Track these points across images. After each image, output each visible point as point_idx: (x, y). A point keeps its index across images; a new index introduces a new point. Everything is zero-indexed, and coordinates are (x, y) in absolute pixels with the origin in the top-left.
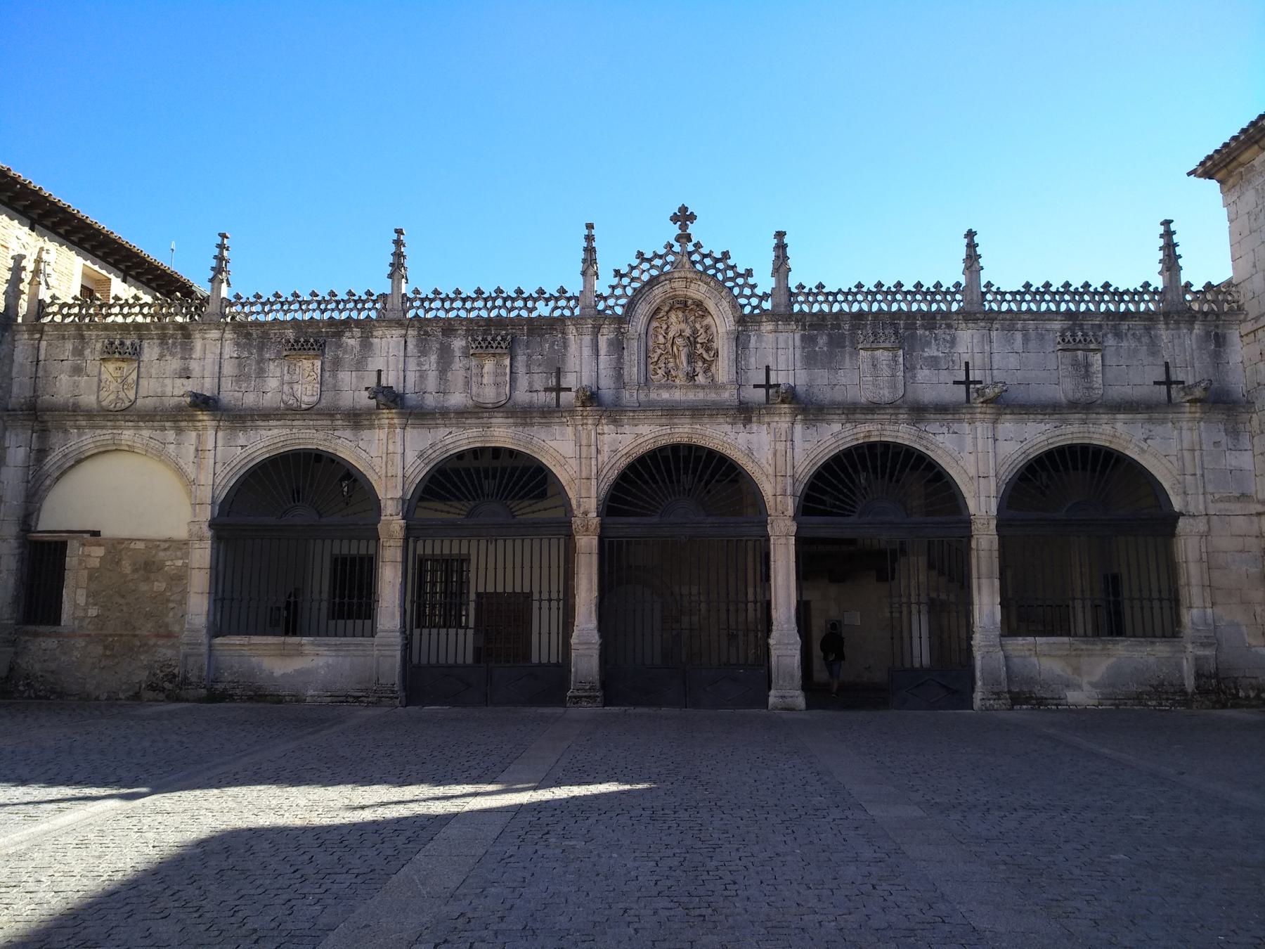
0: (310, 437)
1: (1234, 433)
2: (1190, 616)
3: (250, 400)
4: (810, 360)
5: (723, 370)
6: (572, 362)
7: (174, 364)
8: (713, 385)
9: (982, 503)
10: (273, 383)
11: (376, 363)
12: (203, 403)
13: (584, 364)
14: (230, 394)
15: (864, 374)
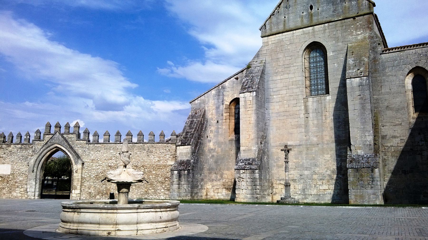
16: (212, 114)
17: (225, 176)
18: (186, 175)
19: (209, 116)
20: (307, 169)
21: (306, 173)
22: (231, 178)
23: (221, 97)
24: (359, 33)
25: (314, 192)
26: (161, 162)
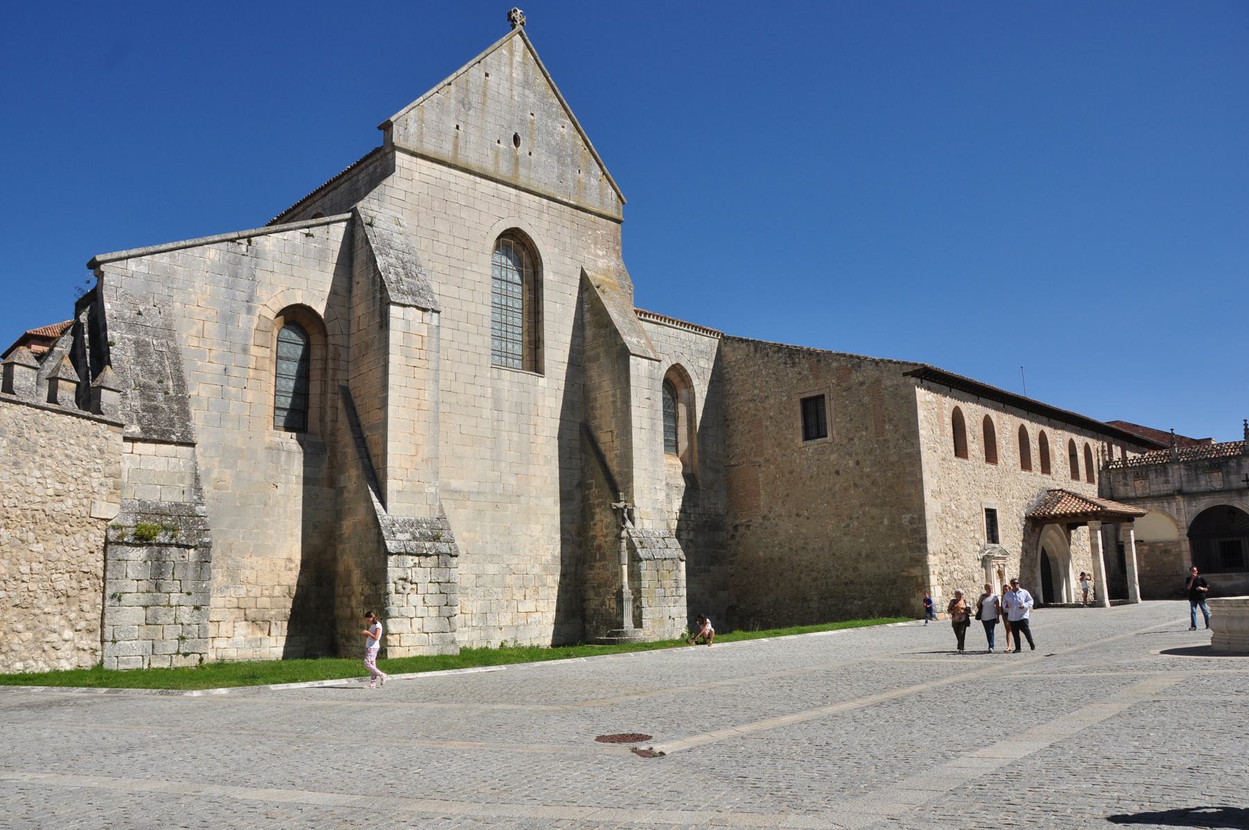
0: (1222, 501)
3: (1195, 489)
7: (1162, 479)
10: (1203, 482)
12: (1180, 492)
14: (1186, 488)
16: (201, 336)
17: (247, 573)
18: (191, 567)
19: (188, 340)
20: (492, 558)
21: (491, 569)
22: (269, 584)
23: (244, 283)
24: (600, 253)
25: (506, 619)
26: (69, 503)
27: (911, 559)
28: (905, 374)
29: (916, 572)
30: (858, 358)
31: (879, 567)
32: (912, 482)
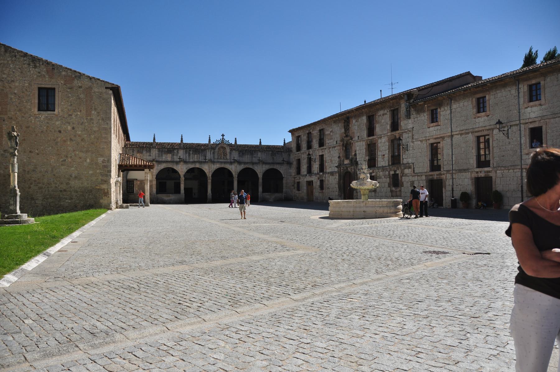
0: (170, 165)
1: (290, 167)
2: (284, 190)
3: (160, 160)
4: (240, 156)
5: (228, 157)
6: (207, 155)
7: (148, 154)
8: (227, 159)
9: (260, 176)
11: (179, 155)
13: (209, 155)
14: (157, 159)
15: (247, 158)
27: (102, 180)
28: (106, 88)
29: (104, 186)
30: (80, 73)
31: (82, 183)
32: (106, 142)
